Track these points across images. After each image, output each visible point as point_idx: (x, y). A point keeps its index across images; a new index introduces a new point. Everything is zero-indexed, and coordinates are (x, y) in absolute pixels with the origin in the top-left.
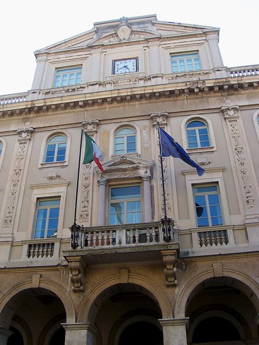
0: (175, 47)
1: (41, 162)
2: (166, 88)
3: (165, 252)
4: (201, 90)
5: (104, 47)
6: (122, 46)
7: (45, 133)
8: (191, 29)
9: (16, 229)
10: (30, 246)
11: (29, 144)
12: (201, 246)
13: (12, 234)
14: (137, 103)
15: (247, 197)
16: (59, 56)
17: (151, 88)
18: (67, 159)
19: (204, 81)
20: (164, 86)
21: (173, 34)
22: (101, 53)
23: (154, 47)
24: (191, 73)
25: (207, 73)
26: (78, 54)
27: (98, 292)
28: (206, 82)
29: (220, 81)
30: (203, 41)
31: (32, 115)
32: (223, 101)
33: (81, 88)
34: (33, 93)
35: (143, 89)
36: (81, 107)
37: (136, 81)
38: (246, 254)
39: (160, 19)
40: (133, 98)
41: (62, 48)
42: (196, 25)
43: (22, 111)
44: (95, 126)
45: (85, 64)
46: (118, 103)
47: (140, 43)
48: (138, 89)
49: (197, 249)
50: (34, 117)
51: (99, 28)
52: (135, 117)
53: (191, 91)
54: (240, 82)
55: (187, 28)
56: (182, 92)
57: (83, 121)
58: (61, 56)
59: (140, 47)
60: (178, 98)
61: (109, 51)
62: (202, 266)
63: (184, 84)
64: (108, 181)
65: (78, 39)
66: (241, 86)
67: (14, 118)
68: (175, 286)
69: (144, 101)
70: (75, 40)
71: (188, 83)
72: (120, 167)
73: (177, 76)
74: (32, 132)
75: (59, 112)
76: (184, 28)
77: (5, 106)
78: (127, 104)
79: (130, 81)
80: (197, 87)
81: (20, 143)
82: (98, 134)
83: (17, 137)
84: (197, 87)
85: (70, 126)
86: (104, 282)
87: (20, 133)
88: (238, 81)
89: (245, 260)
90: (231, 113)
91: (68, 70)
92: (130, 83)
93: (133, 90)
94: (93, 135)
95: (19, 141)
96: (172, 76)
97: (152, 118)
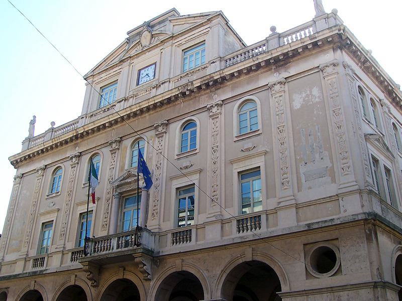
0: (187, 42)
1: (177, 152)
2: (33, 150)
3: (136, 255)
4: (192, 91)
5: (132, 58)
6: (145, 53)
7: (178, 122)
8: (199, 18)
9: (162, 220)
10: (73, 253)
11: (165, 137)
12: (239, 232)
13: (159, 225)
14: (147, 114)
15: (154, 210)
16: (100, 77)
17: (153, 99)
18: (198, 147)
19: (192, 83)
20: (162, 95)
21: (187, 27)
22: (172, 46)
23: (167, 48)
24: (192, 71)
25: (205, 68)
26: (115, 70)
27: (106, 287)
28: (194, 82)
29: (205, 78)
30: (207, 30)
31: (79, 141)
32: (211, 98)
33: (113, 106)
34: (82, 118)
35: (147, 102)
36: (108, 127)
37: (151, 90)
38: (199, 251)
39: (183, 12)
40: (142, 111)
41: (103, 68)
42: (202, 13)
43: (71, 139)
44: (118, 144)
45: (119, 78)
46: (237, 78)
47: (204, 24)
48: (144, 103)
49: (169, 248)
50: (81, 142)
51: (134, 37)
52: (145, 129)
53: (184, 94)
54: (222, 75)
55: (195, 18)
56: (176, 97)
57: (109, 140)
58: (103, 75)
59: (157, 50)
60: (176, 103)
61: (135, 61)
62: (170, 261)
63: (177, 89)
64: (121, 193)
65: (114, 55)
66: (224, 79)
67: (101, 132)
68: (149, 280)
69: (151, 112)
70: (112, 56)
71: (180, 88)
72: (126, 181)
73: (181, 77)
74: (79, 156)
75: (165, 107)
76: (193, 18)
77: (60, 137)
78: (140, 117)
79: (147, 91)
80: (188, 90)
81: (158, 138)
82: (120, 150)
83: (109, 148)
84: (188, 90)
85: (103, 146)
86: (110, 278)
87: (72, 158)
88: (220, 74)
89: (200, 256)
90: (277, 87)
91: (194, 48)
92: (147, 93)
93: (140, 104)
94: (116, 152)
95: (71, 165)
96: (177, 78)
97: (209, 109)
